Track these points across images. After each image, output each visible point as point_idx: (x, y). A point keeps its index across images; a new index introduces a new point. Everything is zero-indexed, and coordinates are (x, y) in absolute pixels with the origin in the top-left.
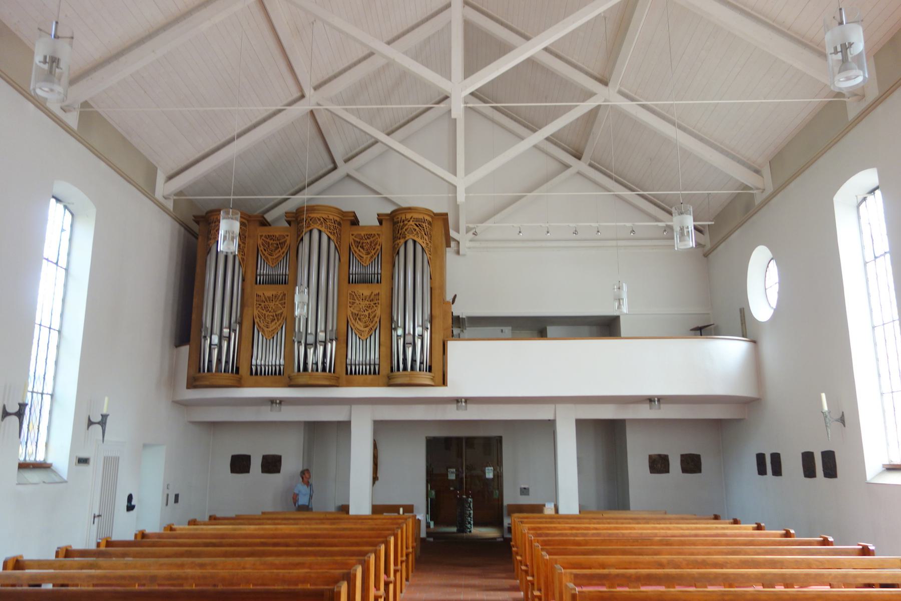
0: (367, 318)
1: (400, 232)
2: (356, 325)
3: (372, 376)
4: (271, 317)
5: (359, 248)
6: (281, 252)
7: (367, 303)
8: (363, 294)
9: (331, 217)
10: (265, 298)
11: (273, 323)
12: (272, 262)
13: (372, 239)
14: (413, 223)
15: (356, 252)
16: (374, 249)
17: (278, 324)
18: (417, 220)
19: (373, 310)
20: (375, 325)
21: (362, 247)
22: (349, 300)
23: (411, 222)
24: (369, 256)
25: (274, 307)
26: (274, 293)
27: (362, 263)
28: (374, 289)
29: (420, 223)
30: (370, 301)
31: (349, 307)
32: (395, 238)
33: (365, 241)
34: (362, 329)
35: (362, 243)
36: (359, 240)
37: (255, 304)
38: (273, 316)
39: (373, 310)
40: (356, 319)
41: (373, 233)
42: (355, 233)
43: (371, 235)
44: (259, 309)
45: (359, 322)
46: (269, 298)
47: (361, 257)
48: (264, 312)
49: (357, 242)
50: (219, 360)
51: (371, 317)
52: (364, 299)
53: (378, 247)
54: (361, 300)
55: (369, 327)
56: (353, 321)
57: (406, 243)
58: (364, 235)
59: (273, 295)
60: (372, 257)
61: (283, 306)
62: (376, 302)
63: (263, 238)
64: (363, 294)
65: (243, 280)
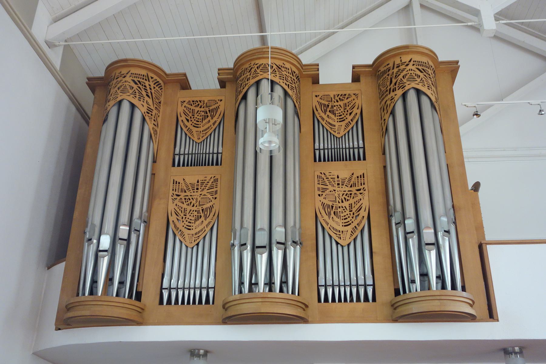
0: (348, 212)
1: (394, 81)
2: (330, 221)
3: (362, 304)
4: (196, 213)
5: (328, 113)
6: (212, 121)
7: (347, 189)
8: (338, 177)
9: (288, 65)
10: (187, 186)
11: (198, 222)
12: (198, 135)
13: (346, 101)
14: (414, 68)
15: (323, 119)
16: (350, 114)
17: (205, 223)
18: (420, 63)
19: (356, 199)
20: (361, 222)
21: (332, 112)
22: (317, 186)
23: (410, 67)
24: (343, 124)
25: (199, 199)
26: (201, 178)
27: (332, 132)
28: (358, 167)
29: (425, 68)
30: (351, 187)
31: (317, 196)
32: (382, 95)
33: (336, 104)
34: (341, 228)
35: (332, 107)
36: (327, 103)
37: (171, 194)
38: (198, 212)
39: (356, 199)
40: (330, 214)
41: (347, 93)
42: (321, 94)
43: (345, 95)
44: (176, 202)
45: (335, 217)
46: (192, 185)
47: (331, 125)
48: (185, 206)
49: (325, 105)
50: (109, 279)
51: (354, 210)
52: (340, 183)
53: (355, 111)
54: (336, 185)
55: (353, 226)
56: (326, 217)
57: (404, 96)
58: (334, 96)
59: (198, 182)
60: (347, 125)
61: (214, 197)
62: (361, 187)
63: (185, 104)
64: (338, 177)
65: (154, 161)
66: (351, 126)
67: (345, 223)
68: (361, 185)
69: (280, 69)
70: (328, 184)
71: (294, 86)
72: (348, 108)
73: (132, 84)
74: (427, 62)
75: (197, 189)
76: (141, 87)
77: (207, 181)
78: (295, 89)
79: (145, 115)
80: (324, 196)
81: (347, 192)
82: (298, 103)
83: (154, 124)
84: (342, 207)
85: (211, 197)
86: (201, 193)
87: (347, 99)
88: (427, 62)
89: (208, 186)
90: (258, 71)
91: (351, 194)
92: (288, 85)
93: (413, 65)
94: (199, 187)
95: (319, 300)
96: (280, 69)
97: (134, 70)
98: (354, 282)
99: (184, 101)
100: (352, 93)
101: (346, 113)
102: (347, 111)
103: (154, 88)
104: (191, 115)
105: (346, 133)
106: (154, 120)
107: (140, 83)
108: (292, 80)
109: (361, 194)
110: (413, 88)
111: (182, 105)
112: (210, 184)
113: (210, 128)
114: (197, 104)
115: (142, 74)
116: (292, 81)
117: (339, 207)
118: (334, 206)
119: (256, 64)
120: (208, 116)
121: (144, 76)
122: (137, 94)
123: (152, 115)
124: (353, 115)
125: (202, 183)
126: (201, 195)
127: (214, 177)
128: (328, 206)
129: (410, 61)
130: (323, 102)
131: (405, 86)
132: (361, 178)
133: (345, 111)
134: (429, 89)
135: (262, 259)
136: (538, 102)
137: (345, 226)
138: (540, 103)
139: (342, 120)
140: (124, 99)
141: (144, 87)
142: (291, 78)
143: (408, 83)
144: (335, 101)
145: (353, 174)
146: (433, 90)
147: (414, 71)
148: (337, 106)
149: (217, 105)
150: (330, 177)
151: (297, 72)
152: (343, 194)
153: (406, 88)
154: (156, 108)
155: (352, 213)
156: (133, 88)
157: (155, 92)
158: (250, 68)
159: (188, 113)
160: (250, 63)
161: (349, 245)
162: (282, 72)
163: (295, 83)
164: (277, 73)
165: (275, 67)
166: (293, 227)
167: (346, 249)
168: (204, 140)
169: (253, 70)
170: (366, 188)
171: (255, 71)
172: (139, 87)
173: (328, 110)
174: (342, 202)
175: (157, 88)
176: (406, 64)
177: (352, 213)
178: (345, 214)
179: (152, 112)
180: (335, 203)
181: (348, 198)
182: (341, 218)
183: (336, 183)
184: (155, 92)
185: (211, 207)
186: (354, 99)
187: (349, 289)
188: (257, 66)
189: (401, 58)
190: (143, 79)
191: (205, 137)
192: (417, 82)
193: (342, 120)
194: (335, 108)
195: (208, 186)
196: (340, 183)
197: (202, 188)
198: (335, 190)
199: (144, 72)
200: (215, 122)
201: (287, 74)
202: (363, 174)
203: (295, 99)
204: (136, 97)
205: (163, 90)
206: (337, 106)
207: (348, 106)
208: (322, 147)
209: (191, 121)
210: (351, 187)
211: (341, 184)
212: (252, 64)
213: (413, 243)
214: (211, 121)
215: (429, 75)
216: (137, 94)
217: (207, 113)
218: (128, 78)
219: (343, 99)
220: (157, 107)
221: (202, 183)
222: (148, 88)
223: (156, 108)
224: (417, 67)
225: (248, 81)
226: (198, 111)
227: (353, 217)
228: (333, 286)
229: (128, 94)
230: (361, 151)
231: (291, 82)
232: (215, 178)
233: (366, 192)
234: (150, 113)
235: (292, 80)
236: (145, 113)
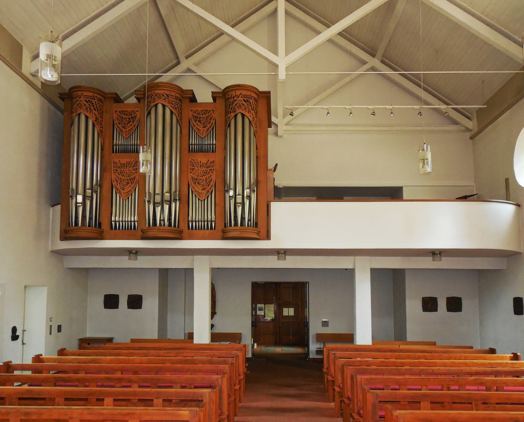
0: (205, 182)
1: (231, 107)
2: (195, 187)
3: (209, 231)
4: (126, 181)
5: (197, 122)
6: (133, 125)
7: (205, 169)
8: (201, 162)
9: (173, 94)
10: (121, 165)
11: (128, 186)
12: (126, 133)
13: (207, 115)
14: (242, 99)
15: (194, 126)
16: (210, 123)
17: (132, 186)
18: (246, 96)
19: (209, 175)
20: (211, 188)
21: (200, 121)
22: (189, 167)
23: (240, 98)
24: (205, 129)
25: (128, 173)
26: (128, 160)
27: (199, 135)
28: (211, 157)
29: (248, 99)
30: (207, 168)
31: (189, 172)
32: (227, 113)
33: (202, 116)
34: (201, 191)
35: (200, 118)
36: (197, 115)
37: (113, 169)
38: (128, 180)
39: (209, 175)
40: (195, 183)
41: (209, 109)
42: (194, 109)
43: (207, 110)
44: (116, 174)
45: (198, 185)
46: (124, 164)
47: (199, 130)
48: (120, 176)
49: (195, 116)
50: (84, 216)
51: (208, 181)
52: (202, 165)
53: (212, 121)
54: (199, 167)
55: (206, 190)
56: (193, 185)
57: (236, 116)
58: (201, 111)
59: (127, 162)
60: (207, 130)
61: (136, 171)
62: (212, 168)
63: (117, 113)
64: (201, 162)
65: (102, 150)
66: (209, 131)
67: (203, 188)
68: (212, 167)
69: (168, 96)
70: (195, 166)
71: (177, 107)
72: (208, 119)
73: (85, 103)
74: (250, 95)
75: (127, 167)
76: (90, 104)
77: (132, 162)
78: (177, 109)
79: (94, 122)
80: (193, 173)
81: (205, 171)
82: (180, 117)
83: (100, 127)
84: (202, 179)
85: (134, 172)
86: (129, 169)
87: (208, 113)
88: (250, 95)
89: (132, 165)
90: (156, 98)
91: (207, 172)
92: (173, 107)
93: (242, 97)
94: (128, 166)
95: (189, 229)
96: (168, 96)
97: (85, 93)
98: (206, 219)
99: (117, 111)
100: (211, 109)
101: (207, 122)
102: (208, 121)
103: (98, 103)
104: (121, 120)
105: (209, 133)
106: (100, 124)
107: (90, 102)
108: (176, 102)
109: (212, 172)
110: (241, 113)
111: (116, 113)
112: (133, 164)
113: (132, 129)
114: (124, 113)
115: (91, 95)
116: (175, 103)
117: (201, 180)
118: (198, 179)
119: (155, 93)
120: (131, 121)
121: (91, 96)
122: (89, 109)
123: (98, 121)
124: (211, 124)
125: (129, 163)
126: (129, 170)
127: (135, 160)
128: (195, 179)
129: (240, 95)
130: (195, 114)
131: (236, 111)
132: (212, 163)
133: (206, 121)
134: (249, 113)
135: (158, 209)
136: (327, 107)
137: (203, 190)
138: (328, 108)
139: (204, 126)
140: (81, 113)
141: (92, 104)
142: (175, 101)
143: (238, 109)
144: (202, 114)
145: (208, 161)
146: (251, 113)
147: (242, 101)
148: (203, 117)
149: (135, 114)
150: (196, 162)
151: (179, 96)
152: (203, 172)
153: (236, 113)
154: (100, 116)
155: (206, 183)
156: (86, 105)
157: (99, 106)
158: (151, 95)
159: (119, 118)
160: (151, 92)
161: (204, 200)
162: (169, 98)
163: (177, 104)
164: (167, 99)
165: (165, 95)
166: (174, 192)
167: (203, 202)
168: (129, 137)
169: (153, 97)
170: (215, 169)
171: (154, 98)
172: (89, 105)
173: (197, 120)
174: (202, 176)
175: (100, 103)
176: (238, 96)
177: (206, 183)
178: (203, 183)
179: (98, 120)
180: (198, 177)
181: (206, 175)
182: (201, 185)
183: (200, 165)
184: (99, 106)
185: (134, 178)
186: (212, 114)
187: (203, 223)
188: (155, 94)
189: (235, 92)
190: (91, 99)
191: (130, 134)
192: (242, 109)
193: (204, 126)
194: (201, 119)
195: (132, 165)
196: (202, 165)
197: (130, 166)
198: (198, 170)
199: (91, 94)
200: (135, 125)
201: (173, 100)
202: (214, 161)
203: (177, 115)
204: (88, 111)
205: (104, 103)
206: (203, 117)
207: (209, 118)
208: (193, 143)
209: (121, 124)
210: (207, 168)
211: (202, 166)
212: (153, 93)
213: (232, 201)
214: (132, 124)
215: (250, 103)
216: (89, 109)
217: (130, 119)
218: (82, 99)
219: (206, 113)
220: (101, 115)
221: (129, 163)
222: (94, 104)
223: (100, 116)
224: (244, 99)
225: (150, 103)
226: (125, 118)
227: (207, 185)
228: (196, 221)
229: (83, 109)
230: (214, 146)
231: (175, 104)
232: (136, 161)
233: (215, 171)
234: (97, 120)
235: (176, 102)
236: (94, 121)
